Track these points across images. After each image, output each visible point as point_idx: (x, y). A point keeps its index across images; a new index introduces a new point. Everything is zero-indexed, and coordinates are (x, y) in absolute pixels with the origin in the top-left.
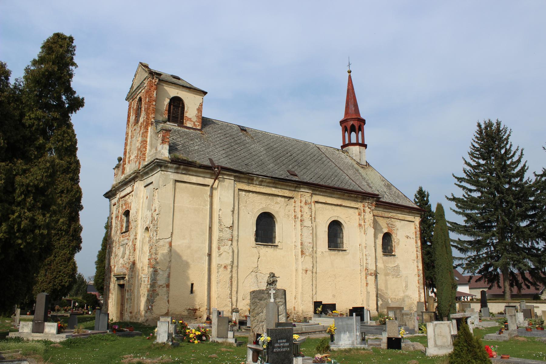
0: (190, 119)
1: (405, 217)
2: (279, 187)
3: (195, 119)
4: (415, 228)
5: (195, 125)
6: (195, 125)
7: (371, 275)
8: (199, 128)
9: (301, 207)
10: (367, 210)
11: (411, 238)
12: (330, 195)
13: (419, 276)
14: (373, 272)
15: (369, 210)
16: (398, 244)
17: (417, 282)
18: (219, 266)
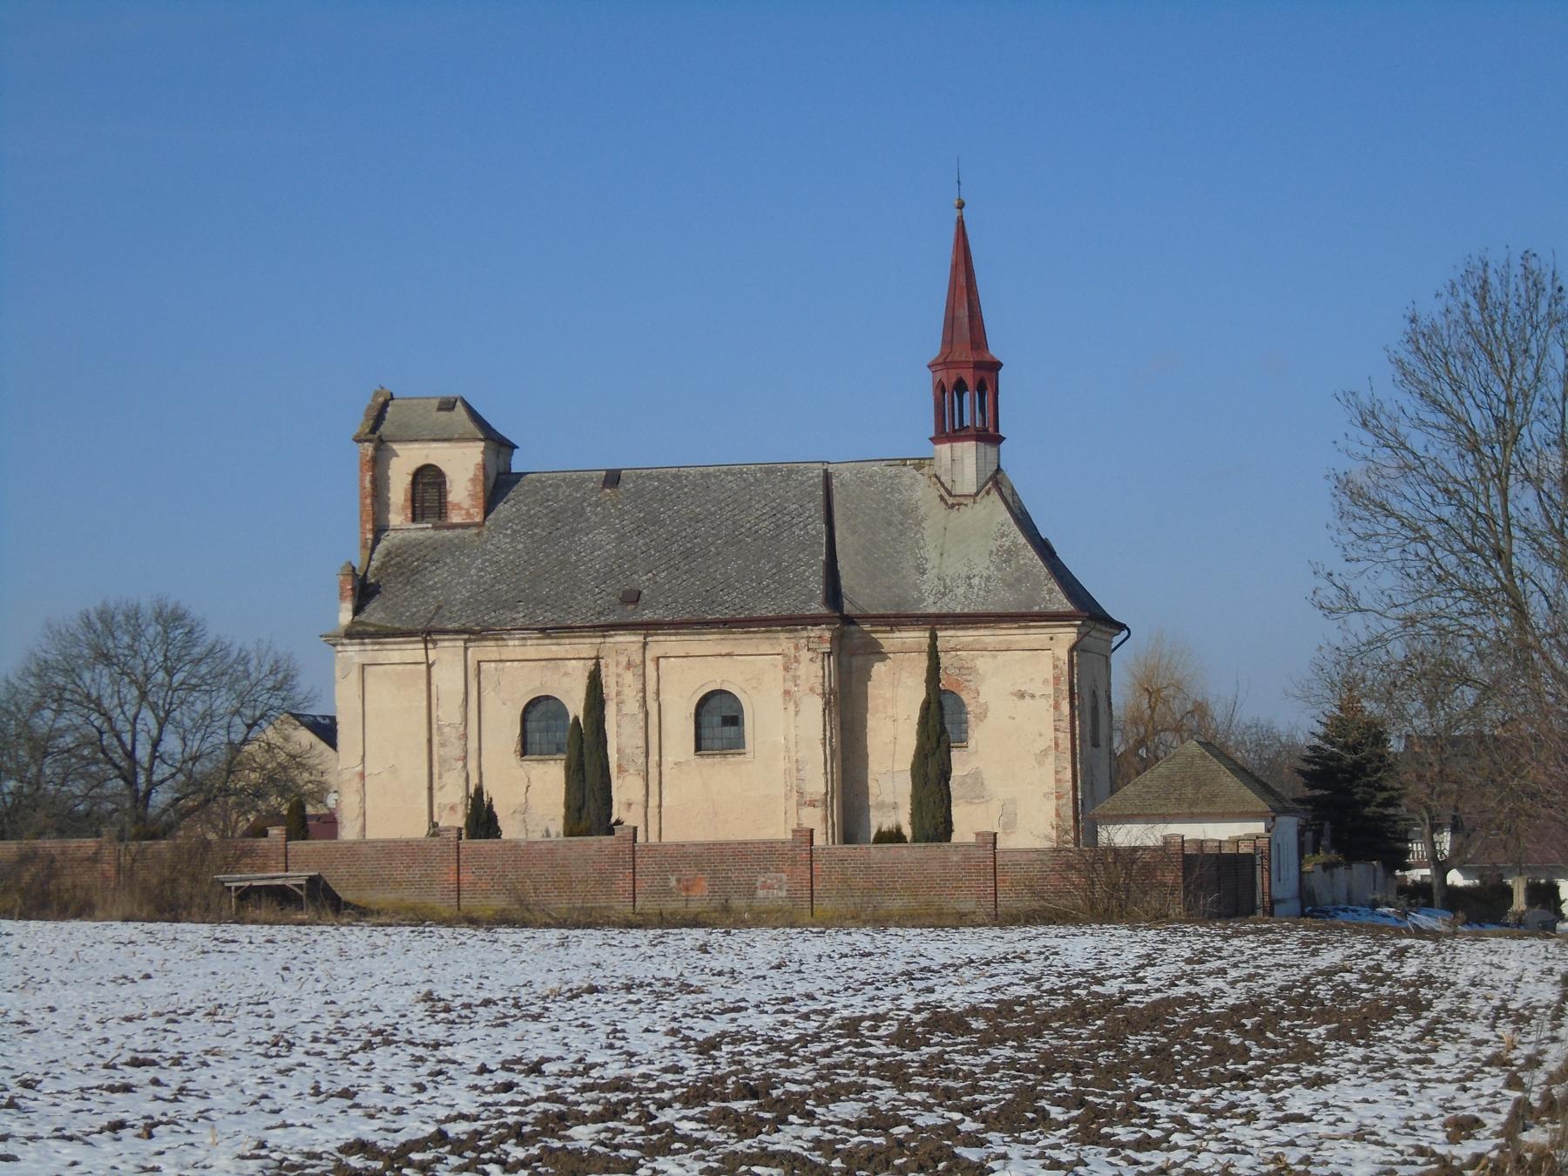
0: (458, 507)
1: (1013, 642)
2: (567, 641)
3: (467, 503)
4: (1055, 667)
5: (468, 514)
6: (468, 514)
7: (812, 804)
8: (478, 519)
9: (618, 675)
10: (805, 655)
11: (1038, 694)
12: (697, 637)
13: (1058, 797)
14: (818, 798)
15: (810, 654)
16: (982, 716)
17: (1054, 812)
18: (442, 807)
